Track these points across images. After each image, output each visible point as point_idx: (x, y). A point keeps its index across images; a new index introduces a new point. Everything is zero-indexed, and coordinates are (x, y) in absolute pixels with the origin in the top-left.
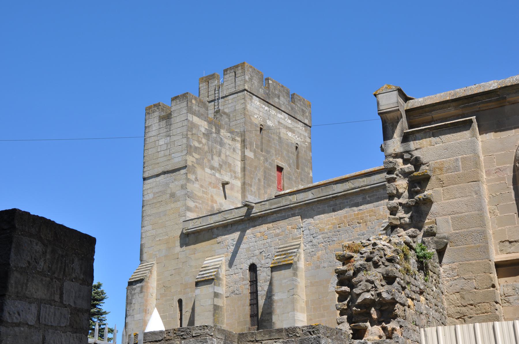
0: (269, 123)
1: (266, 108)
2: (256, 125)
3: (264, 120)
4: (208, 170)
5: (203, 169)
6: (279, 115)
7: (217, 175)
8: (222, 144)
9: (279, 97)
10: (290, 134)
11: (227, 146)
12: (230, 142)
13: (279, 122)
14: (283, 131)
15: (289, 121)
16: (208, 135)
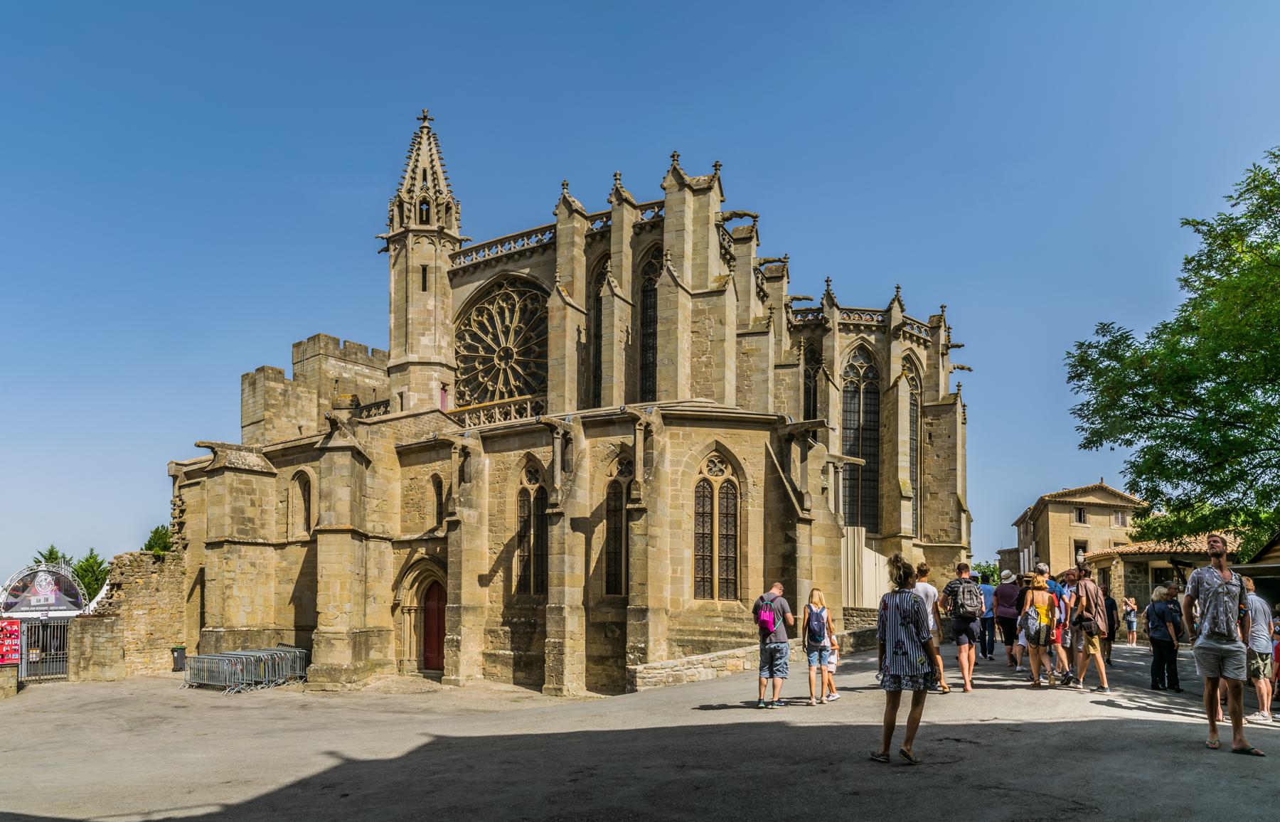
0: (345, 375)
1: (343, 364)
2: (332, 379)
3: (340, 374)
4: (284, 419)
5: (280, 418)
6: (356, 368)
7: (293, 421)
8: (298, 398)
9: (356, 354)
10: (367, 381)
11: (304, 398)
12: (307, 395)
13: (356, 374)
14: (359, 379)
15: (367, 371)
16: (284, 393)
